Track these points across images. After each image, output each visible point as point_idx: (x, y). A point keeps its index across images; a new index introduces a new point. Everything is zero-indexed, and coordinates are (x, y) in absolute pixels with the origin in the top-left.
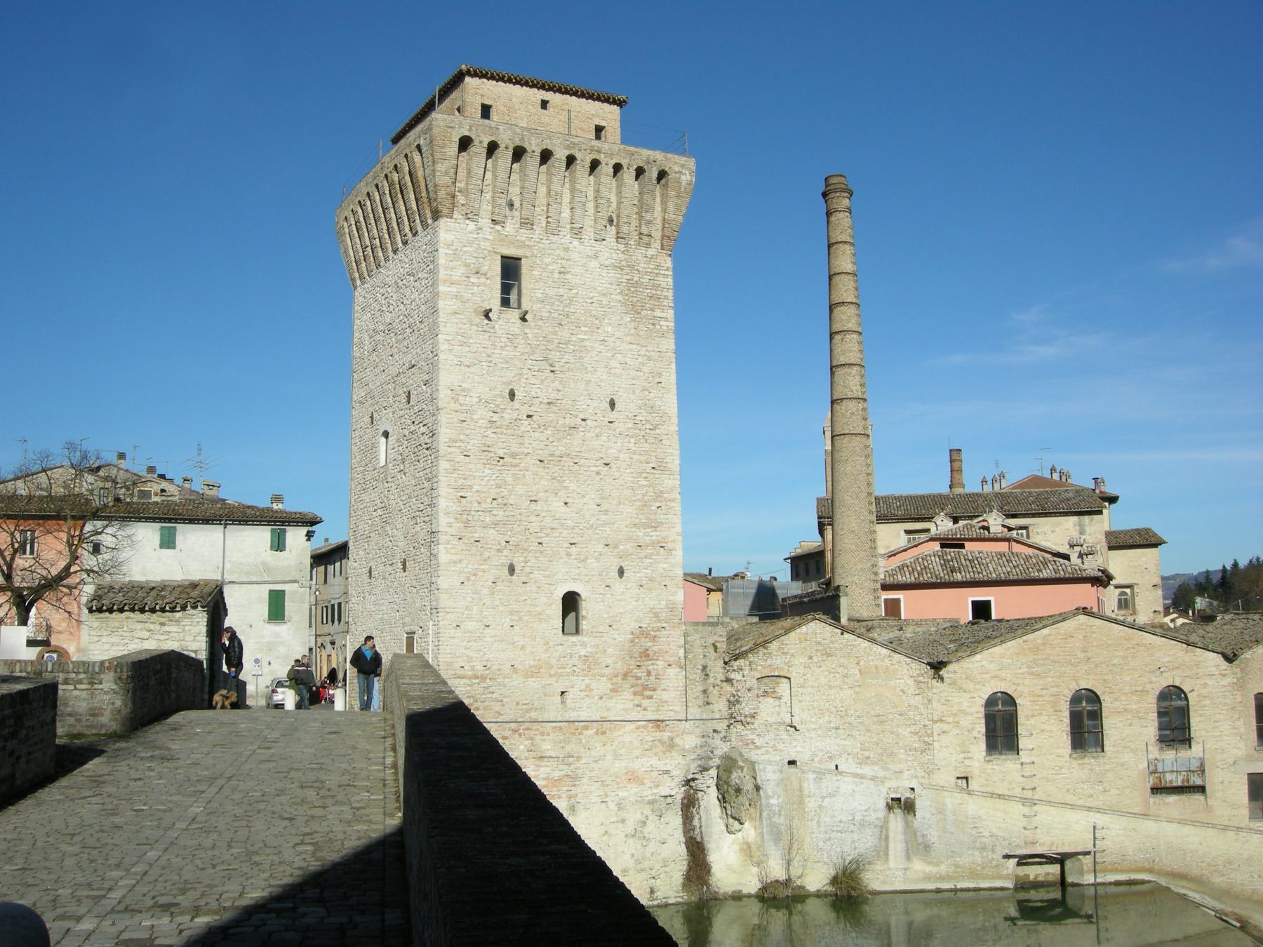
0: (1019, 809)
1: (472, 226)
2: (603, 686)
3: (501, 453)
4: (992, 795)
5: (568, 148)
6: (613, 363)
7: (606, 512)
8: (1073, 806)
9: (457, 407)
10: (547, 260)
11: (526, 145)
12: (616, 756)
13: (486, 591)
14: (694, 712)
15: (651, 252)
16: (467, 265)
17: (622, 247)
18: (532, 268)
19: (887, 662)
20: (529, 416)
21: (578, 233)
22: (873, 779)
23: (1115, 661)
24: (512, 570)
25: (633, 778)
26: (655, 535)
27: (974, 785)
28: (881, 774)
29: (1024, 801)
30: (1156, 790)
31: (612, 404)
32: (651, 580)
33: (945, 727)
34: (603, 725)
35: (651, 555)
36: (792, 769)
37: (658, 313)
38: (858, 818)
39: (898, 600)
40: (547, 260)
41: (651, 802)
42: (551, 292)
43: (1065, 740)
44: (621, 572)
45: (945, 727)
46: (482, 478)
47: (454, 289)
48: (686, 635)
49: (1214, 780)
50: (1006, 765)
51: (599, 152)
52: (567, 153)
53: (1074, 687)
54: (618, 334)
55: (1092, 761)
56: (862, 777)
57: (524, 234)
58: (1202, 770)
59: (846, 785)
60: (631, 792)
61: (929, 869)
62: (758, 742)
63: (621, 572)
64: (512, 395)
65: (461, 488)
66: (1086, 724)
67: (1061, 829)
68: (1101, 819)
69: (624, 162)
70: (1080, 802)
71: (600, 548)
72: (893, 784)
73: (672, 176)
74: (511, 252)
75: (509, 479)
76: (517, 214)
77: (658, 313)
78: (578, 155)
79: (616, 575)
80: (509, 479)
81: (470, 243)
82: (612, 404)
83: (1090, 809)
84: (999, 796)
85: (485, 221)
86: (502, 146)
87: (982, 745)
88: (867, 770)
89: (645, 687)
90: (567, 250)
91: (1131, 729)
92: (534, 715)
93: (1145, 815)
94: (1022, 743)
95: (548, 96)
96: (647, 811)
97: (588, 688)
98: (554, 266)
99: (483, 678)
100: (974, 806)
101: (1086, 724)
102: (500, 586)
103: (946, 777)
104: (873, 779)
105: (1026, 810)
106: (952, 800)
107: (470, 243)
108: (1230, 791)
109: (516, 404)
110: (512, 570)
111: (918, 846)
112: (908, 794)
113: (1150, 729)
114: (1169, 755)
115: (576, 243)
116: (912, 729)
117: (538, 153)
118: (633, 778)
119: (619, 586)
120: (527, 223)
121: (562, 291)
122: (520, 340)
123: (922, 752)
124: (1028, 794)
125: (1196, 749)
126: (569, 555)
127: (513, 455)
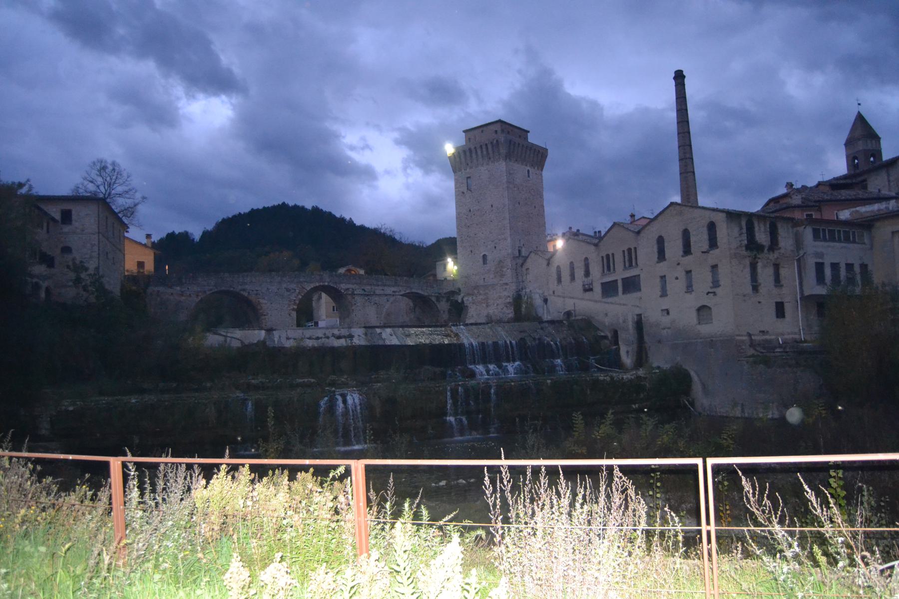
0: (562, 299)
2: (492, 276)
14: (515, 280)
30: (586, 290)
49: (595, 284)
50: (560, 287)
58: (592, 284)
60: (499, 301)
67: (569, 305)
68: (576, 301)
91: (580, 273)
93: (582, 299)
103: (551, 292)
108: (598, 289)
113: (583, 273)
114: (586, 280)
120: (471, 168)
125: (591, 278)
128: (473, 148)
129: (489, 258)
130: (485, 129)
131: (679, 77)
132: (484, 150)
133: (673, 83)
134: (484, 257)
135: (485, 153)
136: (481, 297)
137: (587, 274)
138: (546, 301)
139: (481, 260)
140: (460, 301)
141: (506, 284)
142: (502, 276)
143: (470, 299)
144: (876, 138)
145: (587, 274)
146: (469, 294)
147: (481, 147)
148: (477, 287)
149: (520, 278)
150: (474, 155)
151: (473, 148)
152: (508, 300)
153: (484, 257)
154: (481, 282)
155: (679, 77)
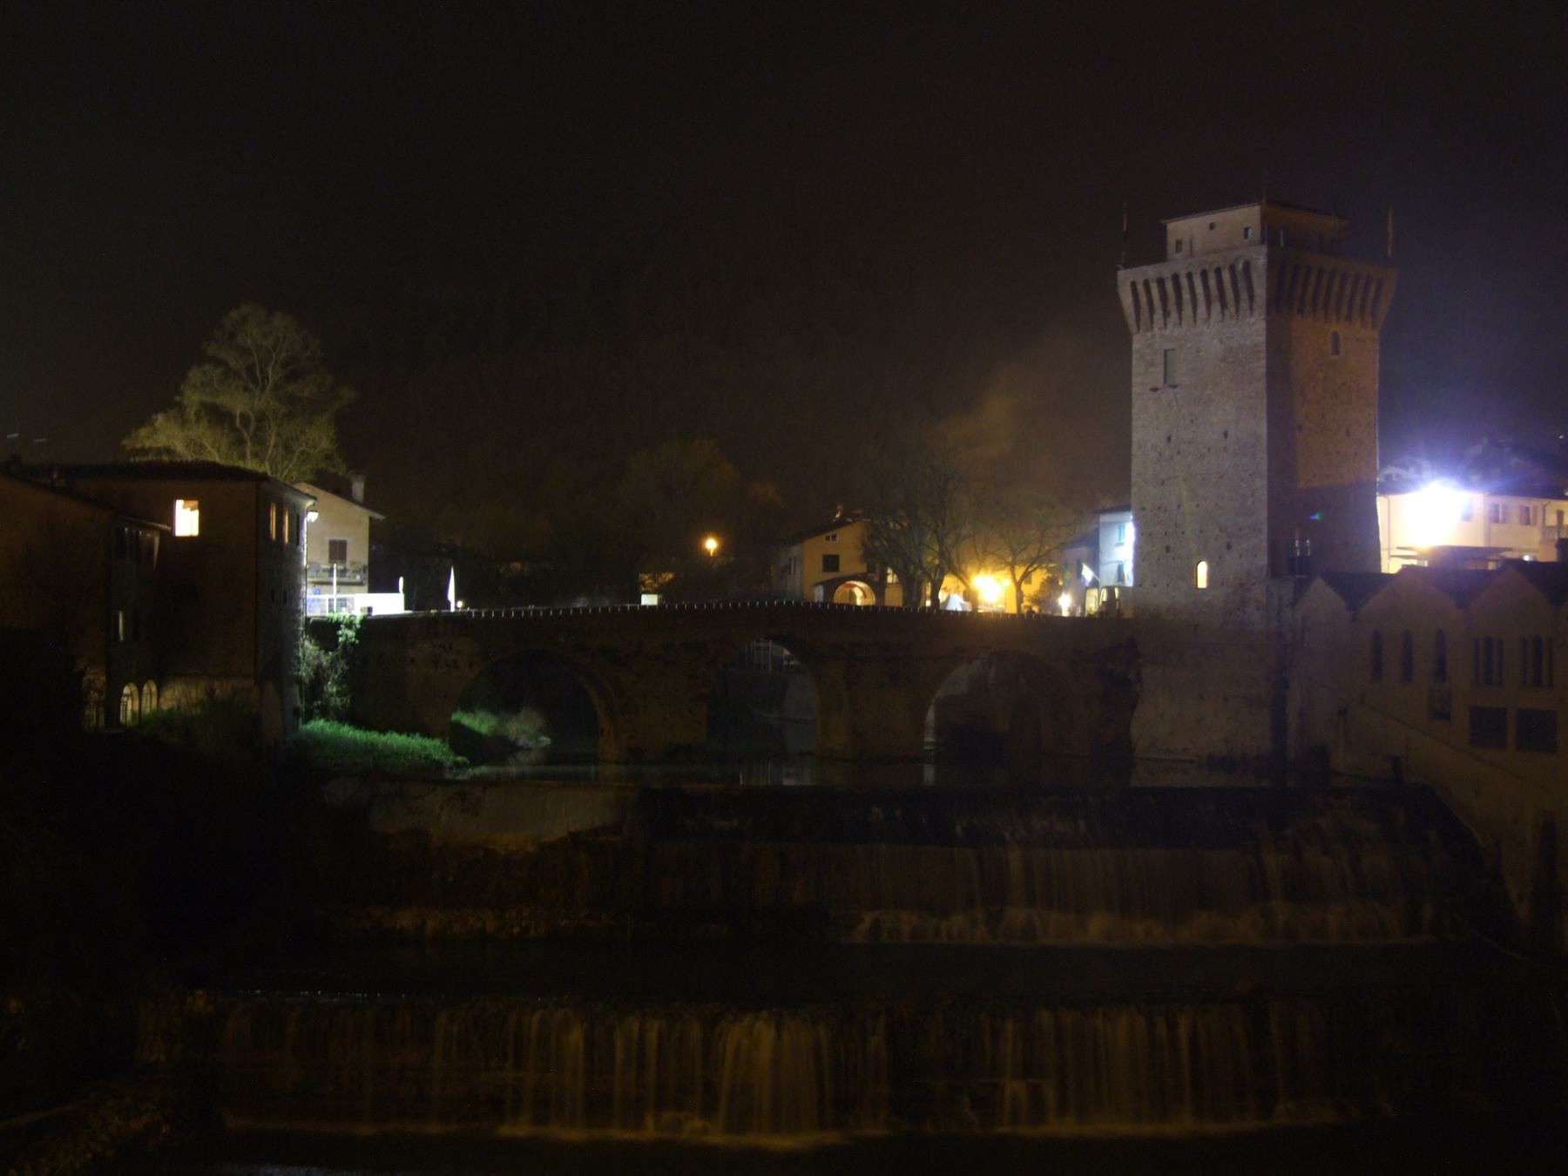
24: (1168, 549)
31: (1226, 435)
44: (1229, 547)
63: (1229, 547)
64: (1169, 439)
74: (1168, 346)
132: (1212, 282)
137: (1441, 670)
138: (1343, 712)
140: (1131, 676)
145: (1441, 670)
150: (1186, 296)
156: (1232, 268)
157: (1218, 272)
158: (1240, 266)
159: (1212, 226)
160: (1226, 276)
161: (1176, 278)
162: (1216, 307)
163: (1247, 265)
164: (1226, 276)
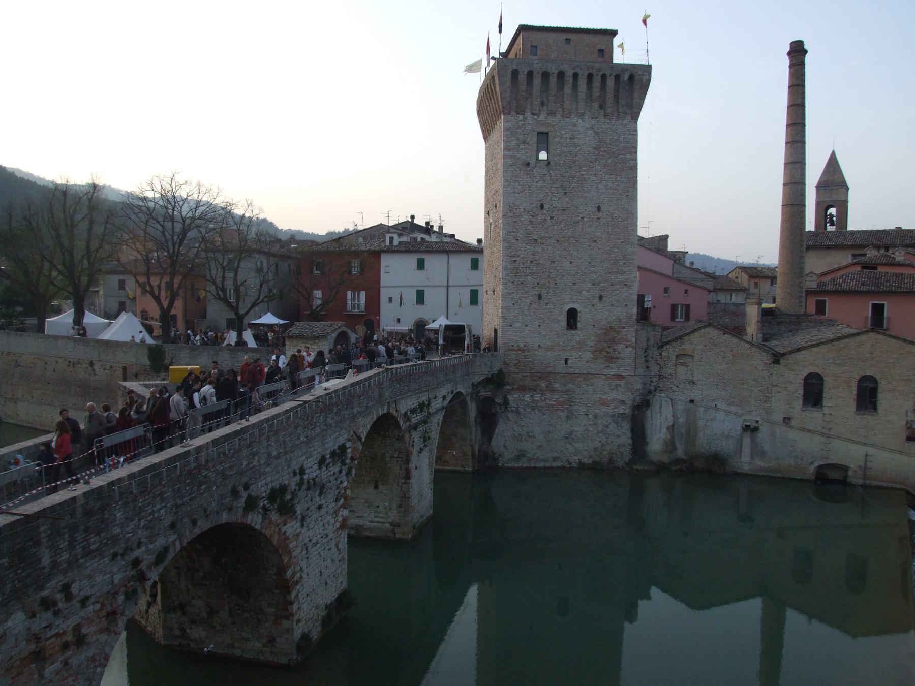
1: (521, 117)
2: (588, 356)
3: (535, 237)
4: (804, 430)
5: (574, 68)
6: (600, 186)
7: (594, 266)
8: (853, 441)
9: (511, 214)
10: (563, 132)
11: (550, 71)
12: (594, 391)
13: (526, 308)
14: (641, 371)
15: (625, 122)
16: (518, 139)
17: (608, 121)
18: (554, 138)
19: (749, 352)
20: (552, 218)
21: (581, 116)
22: (735, 414)
23: (891, 361)
24: (540, 297)
25: (604, 403)
26: (621, 278)
27: (794, 423)
28: (740, 412)
29: (823, 435)
31: (599, 209)
32: (618, 301)
33: (779, 390)
34: (587, 377)
35: (618, 289)
36: (691, 405)
37: (628, 156)
38: (726, 433)
39: (825, 301)
40: (563, 132)
41: (613, 416)
42: (564, 149)
43: (853, 405)
44: (601, 298)
45: (779, 390)
46: (525, 250)
47: (511, 153)
48: (637, 331)
51: (593, 68)
52: (572, 71)
53: (862, 373)
54: (604, 170)
55: (869, 418)
56: (729, 412)
57: (550, 120)
59: (721, 415)
61: (763, 464)
62: (674, 388)
63: (601, 298)
64: (542, 207)
65: (512, 257)
66: (867, 395)
68: (871, 451)
69: (608, 72)
70: (859, 439)
71: (589, 285)
72: (747, 417)
73: (637, 77)
74: (544, 129)
75: (540, 250)
76: (545, 108)
77: (628, 156)
78: (580, 72)
79: (597, 299)
80: (540, 250)
81: (520, 127)
82: (599, 209)
83: (864, 444)
84: (809, 431)
85: (528, 115)
86: (535, 73)
87: (801, 402)
88: (733, 409)
89: (612, 358)
90: (575, 125)
92: (550, 370)
94: (826, 402)
95: (569, 36)
96: (610, 420)
97: (580, 357)
98: (567, 135)
99: (523, 351)
100: (792, 434)
101: (867, 395)
102: (534, 306)
103: (778, 417)
104: (735, 414)
105: (823, 439)
106: (780, 430)
107: (520, 127)
109: (545, 212)
110: (540, 297)
111: (757, 451)
112: (755, 424)
115: (580, 121)
116: (760, 389)
117: (556, 75)
118: (604, 403)
119: (599, 305)
120: (552, 113)
121: (571, 149)
122: (548, 177)
123: (765, 402)
124: (826, 432)
126: (572, 289)
127: (543, 238)
128: (569, 73)
129: (584, 318)
130: (574, 37)
131: (797, 52)
132: (597, 84)
133: (786, 61)
134: (572, 316)
135: (596, 92)
136: (556, 397)
139: (563, 319)
141: (620, 377)
142: (611, 359)
143: (527, 397)
144: (844, 187)
146: (523, 389)
147: (590, 77)
148: (545, 375)
149: (654, 369)
150: (568, 90)
151: (569, 73)
152: (622, 409)
153: (572, 316)
154: (561, 367)
155: (797, 52)
156: (617, 77)
157: (604, 77)
158: (626, 77)
159: (568, 40)
160: (611, 83)
161: (561, 75)
162: (596, 105)
163: (631, 78)
164: (611, 83)
